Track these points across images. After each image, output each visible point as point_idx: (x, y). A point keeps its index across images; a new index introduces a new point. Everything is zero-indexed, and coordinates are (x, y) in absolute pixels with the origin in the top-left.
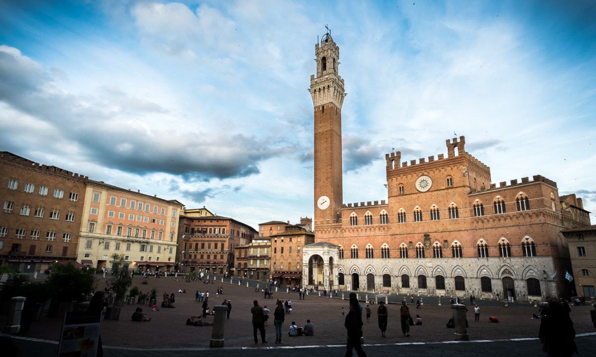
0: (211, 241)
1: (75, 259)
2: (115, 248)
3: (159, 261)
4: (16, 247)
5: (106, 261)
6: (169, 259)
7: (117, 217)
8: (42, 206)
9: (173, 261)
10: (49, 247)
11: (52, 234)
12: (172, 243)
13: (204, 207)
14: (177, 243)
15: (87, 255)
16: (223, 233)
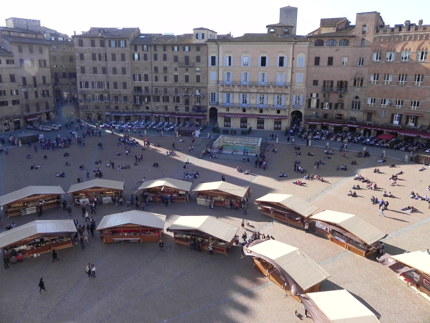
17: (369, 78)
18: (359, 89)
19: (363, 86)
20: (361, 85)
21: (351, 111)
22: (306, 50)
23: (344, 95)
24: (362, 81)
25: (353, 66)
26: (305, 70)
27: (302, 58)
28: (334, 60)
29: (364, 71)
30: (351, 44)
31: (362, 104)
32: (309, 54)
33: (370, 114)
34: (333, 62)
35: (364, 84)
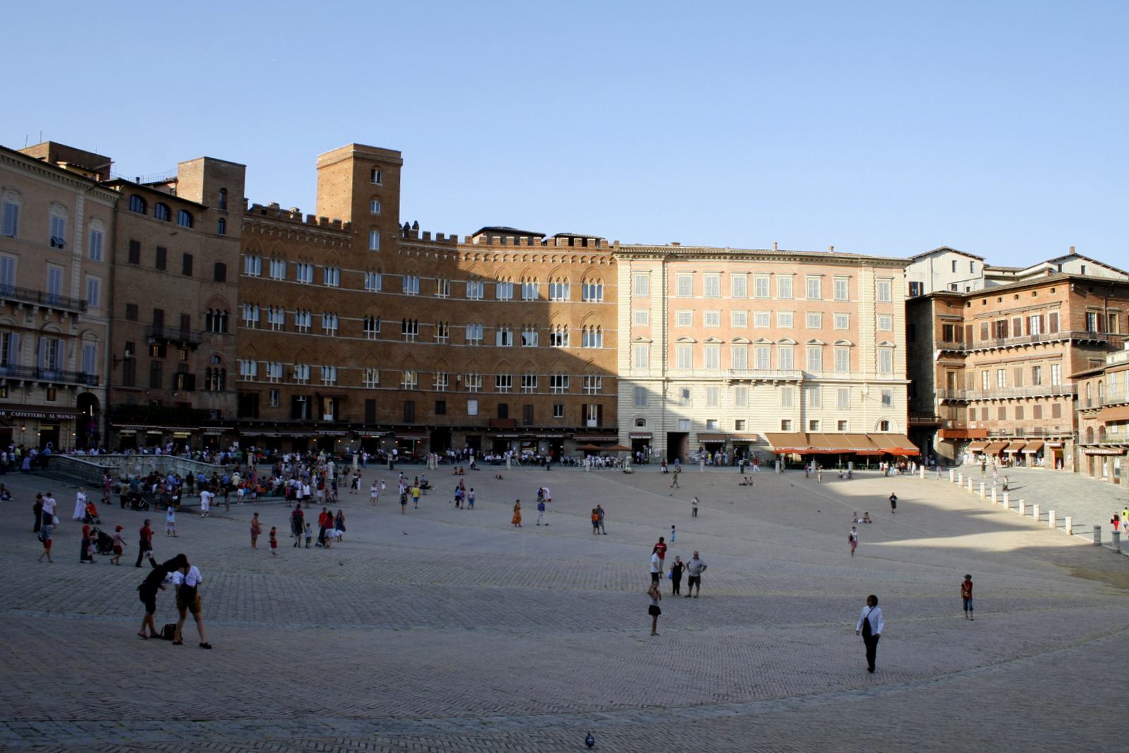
0: (1023, 360)
1: (615, 432)
2: (705, 401)
3: (847, 430)
4: (503, 410)
5: (686, 434)
6: (885, 425)
7: (701, 324)
8: (533, 324)
9: (899, 425)
10: (558, 409)
11: (593, 379)
12: (889, 378)
13: (1073, 248)
14: (908, 378)
15: (640, 423)
16: (1054, 328)
17: (240, 311)
18: (220, 338)
19: (231, 332)
20: (225, 330)
21: (206, 394)
22: (108, 215)
23: (190, 353)
24: (225, 318)
25: (203, 281)
26: (105, 271)
27: (100, 235)
28: (168, 255)
29: (229, 293)
30: (196, 225)
31: (229, 374)
32: (114, 228)
33: (249, 400)
34: (167, 263)
35: (232, 327)
